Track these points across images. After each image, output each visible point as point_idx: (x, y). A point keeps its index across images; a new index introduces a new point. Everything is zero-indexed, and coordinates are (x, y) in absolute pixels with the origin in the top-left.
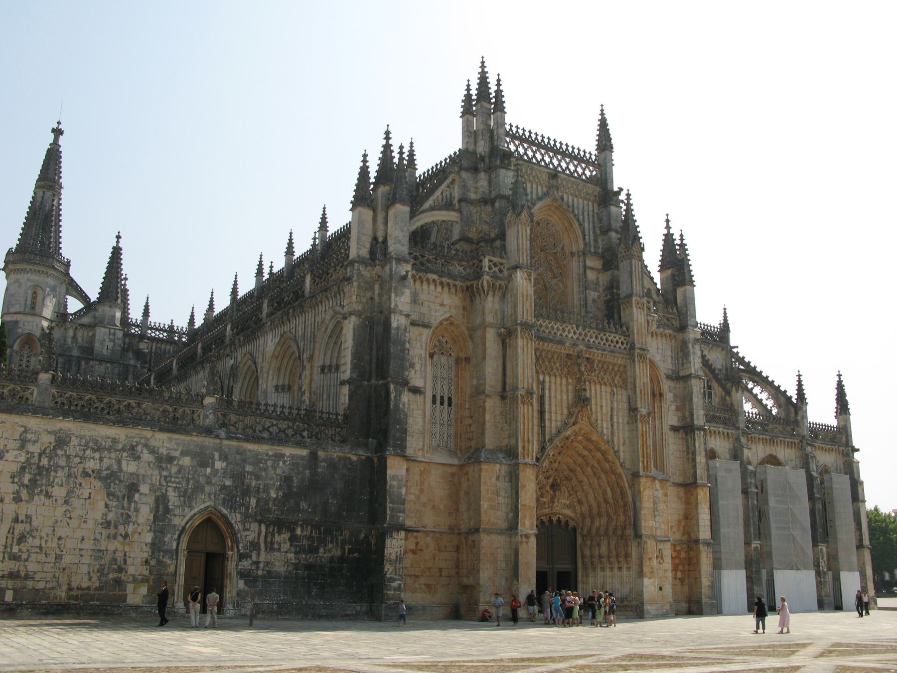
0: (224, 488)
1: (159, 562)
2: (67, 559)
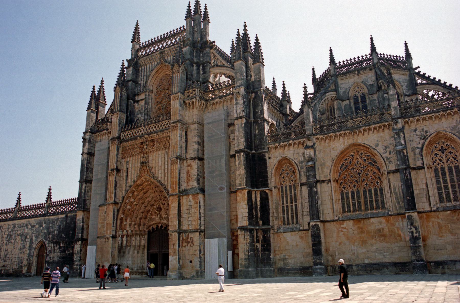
0: (45, 232)
1: (30, 259)
2: (13, 260)
